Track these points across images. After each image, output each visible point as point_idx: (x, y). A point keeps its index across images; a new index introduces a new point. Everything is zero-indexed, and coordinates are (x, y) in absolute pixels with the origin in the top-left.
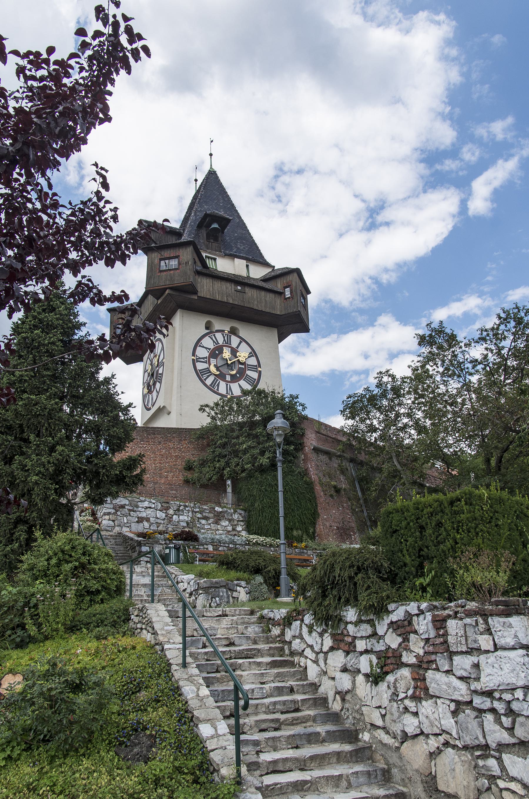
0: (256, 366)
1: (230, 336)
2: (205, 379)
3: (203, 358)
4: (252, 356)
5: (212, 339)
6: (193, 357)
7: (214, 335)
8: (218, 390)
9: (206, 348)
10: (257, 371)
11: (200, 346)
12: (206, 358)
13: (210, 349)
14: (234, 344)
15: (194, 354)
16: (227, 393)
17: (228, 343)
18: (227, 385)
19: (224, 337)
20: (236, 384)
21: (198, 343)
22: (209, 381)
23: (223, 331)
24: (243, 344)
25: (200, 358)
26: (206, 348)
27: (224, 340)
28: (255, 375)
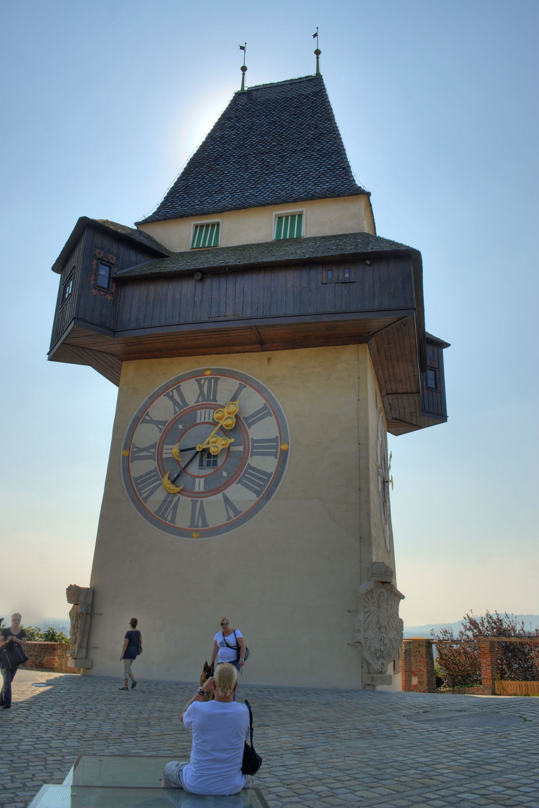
0: (275, 440)
1: (216, 380)
2: (146, 499)
3: (146, 449)
4: (268, 414)
5: (172, 398)
7: (178, 389)
9: (157, 423)
10: (275, 455)
12: (153, 446)
18: (194, 503)
19: (201, 387)
20: (219, 497)
23: (201, 373)
24: (248, 391)
25: (140, 450)
27: (201, 394)
28: (268, 464)
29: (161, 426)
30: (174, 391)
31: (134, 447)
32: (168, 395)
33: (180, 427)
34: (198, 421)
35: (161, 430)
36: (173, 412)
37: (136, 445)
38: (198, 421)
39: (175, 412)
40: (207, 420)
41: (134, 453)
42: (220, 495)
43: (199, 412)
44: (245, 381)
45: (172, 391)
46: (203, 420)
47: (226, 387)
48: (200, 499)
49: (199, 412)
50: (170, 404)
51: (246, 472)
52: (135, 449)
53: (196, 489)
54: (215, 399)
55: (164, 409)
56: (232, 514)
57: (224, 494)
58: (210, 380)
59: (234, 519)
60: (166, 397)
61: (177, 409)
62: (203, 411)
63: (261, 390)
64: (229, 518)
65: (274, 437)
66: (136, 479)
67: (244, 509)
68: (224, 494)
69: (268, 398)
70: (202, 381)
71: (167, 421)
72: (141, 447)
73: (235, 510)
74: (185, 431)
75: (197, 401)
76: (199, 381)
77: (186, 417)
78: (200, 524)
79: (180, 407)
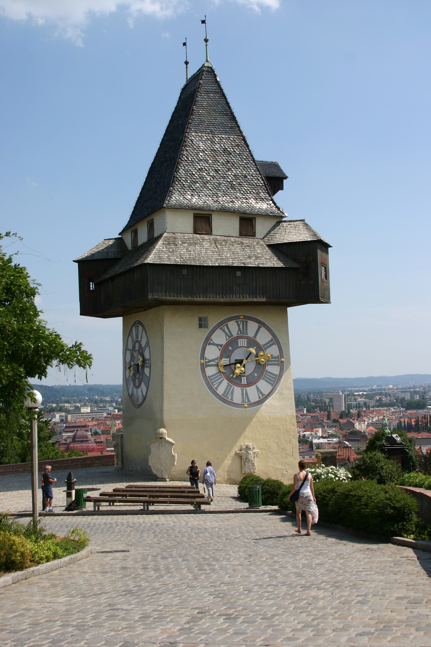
2: (217, 388)
3: (213, 360)
4: (274, 344)
5: (224, 331)
6: (202, 361)
8: (232, 399)
9: (217, 345)
11: (210, 344)
13: (221, 346)
14: (251, 334)
15: (203, 356)
16: (243, 401)
17: (243, 334)
18: (242, 390)
19: (239, 326)
21: (208, 341)
22: (221, 390)
24: (263, 329)
25: (210, 361)
26: (217, 345)
27: (239, 329)
29: (220, 347)
30: (225, 327)
31: (206, 359)
32: (221, 329)
33: (230, 348)
34: (239, 346)
35: (220, 350)
36: (225, 339)
37: (207, 358)
38: (239, 346)
39: (227, 340)
40: (244, 345)
41: (206, 362)
42: (255, 385)
43: (239, 340)
44: (261, 324)
45: (223, 326)
46: (242, 345)
47: (252, 327)
48: (245, 388)
49: (239, 340)
50: (224, 334)
51: (266, 374)
52: (207, 361)
53: (243, 383)
54: (247, 334)
55: (220, 338)
56: (261, 396)
57: (256, 385)
58: (243, 322)
59: (262, 398)
60: (221, 330)
61: (228, 338)
62: (241, 340)
63: (269, 330)
64: (260, 398)
65: (277, 356)
66: (209, 377)
67: (266, 393)
68: (256, 385)
69: (273, 335)
70: (239, 322)
71: (223, 345)
72: (210, 359)
73: (261, 393)
74: (233, 351)
75: (238, 334)
76: (237, 322)
77: (232, 343)
78: (247, 401)
79: (229, 337)
